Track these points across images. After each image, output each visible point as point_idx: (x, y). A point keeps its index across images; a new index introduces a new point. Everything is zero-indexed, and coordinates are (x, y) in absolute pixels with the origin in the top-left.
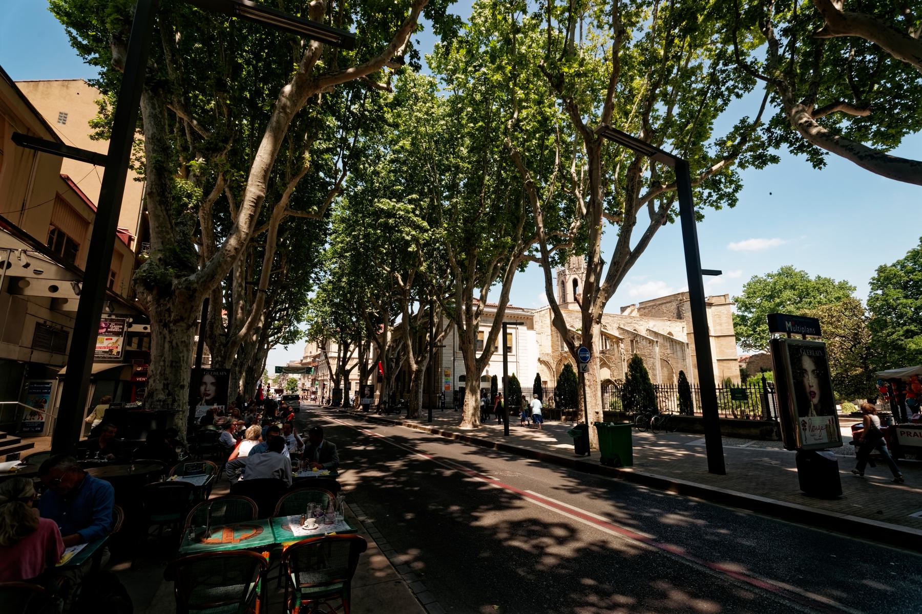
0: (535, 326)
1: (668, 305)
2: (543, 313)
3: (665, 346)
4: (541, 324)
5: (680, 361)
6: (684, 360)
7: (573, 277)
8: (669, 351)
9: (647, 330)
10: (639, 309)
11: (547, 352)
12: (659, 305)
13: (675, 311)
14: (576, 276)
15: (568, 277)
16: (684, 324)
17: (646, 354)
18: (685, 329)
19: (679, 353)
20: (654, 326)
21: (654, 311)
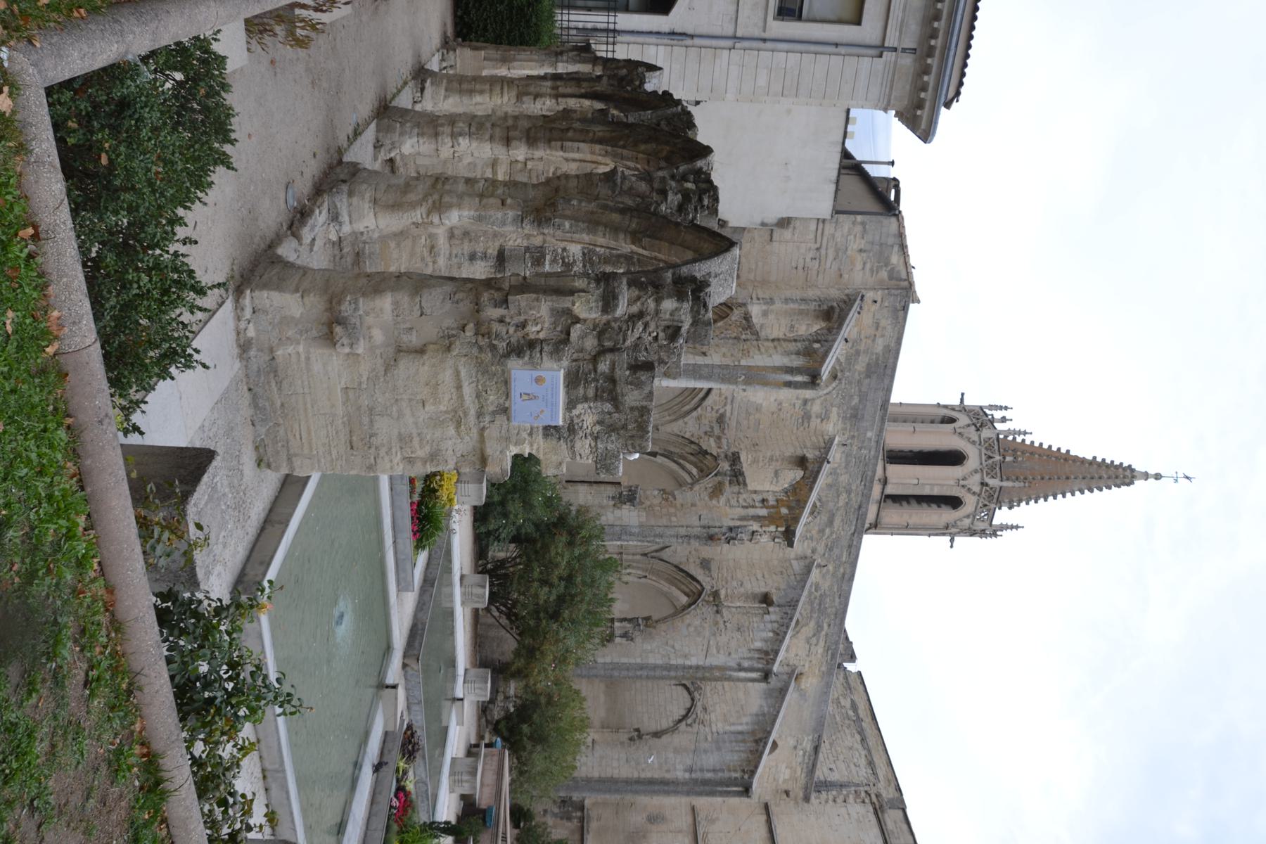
12: (861, 732)
14: (972, 462)
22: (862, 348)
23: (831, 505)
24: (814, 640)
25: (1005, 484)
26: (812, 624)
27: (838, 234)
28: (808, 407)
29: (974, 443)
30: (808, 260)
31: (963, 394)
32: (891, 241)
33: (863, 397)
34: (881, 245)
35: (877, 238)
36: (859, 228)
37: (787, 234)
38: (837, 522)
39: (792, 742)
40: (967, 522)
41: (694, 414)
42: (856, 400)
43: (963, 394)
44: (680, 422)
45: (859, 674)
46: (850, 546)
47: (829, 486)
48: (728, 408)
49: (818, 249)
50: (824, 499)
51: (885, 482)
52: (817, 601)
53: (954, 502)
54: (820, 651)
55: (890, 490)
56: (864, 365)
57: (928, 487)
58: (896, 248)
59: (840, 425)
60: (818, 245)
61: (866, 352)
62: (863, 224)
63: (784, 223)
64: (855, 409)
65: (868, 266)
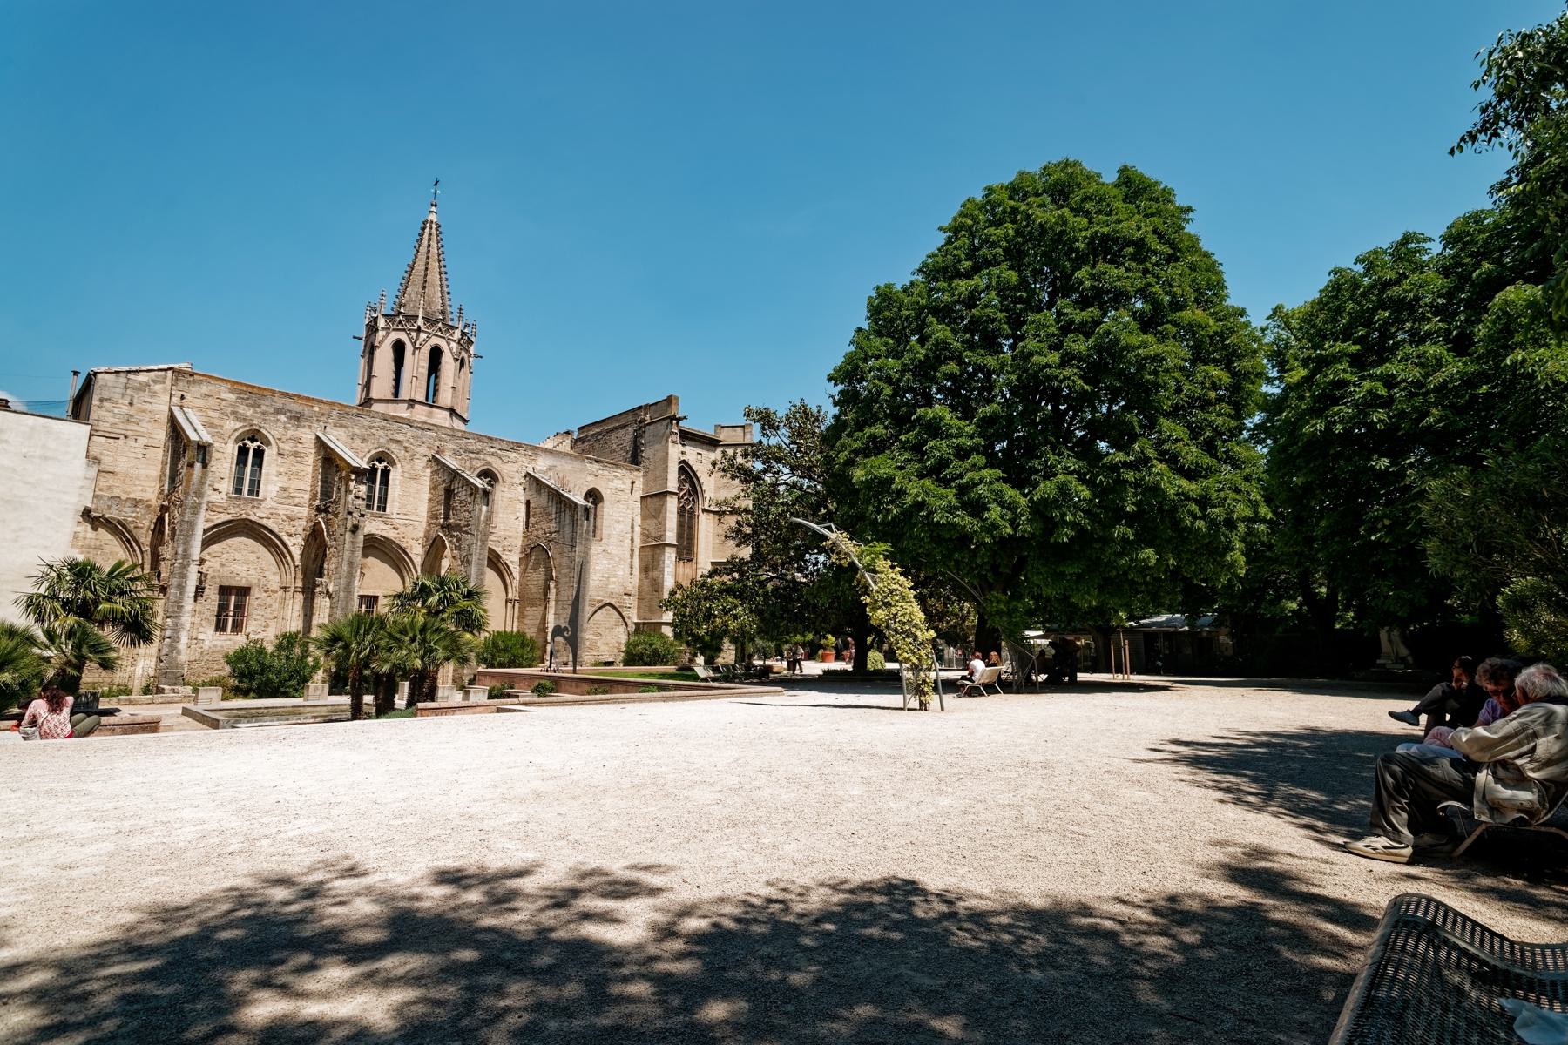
0: (95, 413)
1: (621, 432)
2: (142, 378)
3: (549, 514)
4: (126, 409)
5: (567, 549)
6: (573, 546)
7: (394, 336)
8: (553, 527)
9: (528, 475)
10: (574, 443)
11: (137, 495)
12: (609, 431)
13: (630, 448)
14: (403, 336)
15: (381, 334)
16: (638, 477)
17: (463, 523)
18: (639, 485)
19: (568, 530)
20: (551, 468)
21: (597, 446)
22: (230, 409)
23: (381, 440)
24: (505, 459)
25: (421, 315)
26: (489, 459)
27: (112, 420)
28: (285, 453)
29: (388, 334)
30: (136, 445)
31: (354, 337)
32: (122, 379)
33: (278, 411)
34: (126, 388)
35: (118, 390)
36: (107, 404)
37: (105, 460)
38: (400, 437)
39: (590, 478)
40: (454, 345)
41: (286, 538)
42: (283, 418)
43: (354, 337)
44: (292, 549)
45: (579, 429)
46: (423, 429)
47: (364, 440)
48: (281, 512)
49: (126, 437)
50: (376, 446)
51: (412, 403)
52: (470, 455)
53: (436, 354)
54: (515, 455)
55: (421, 397)
56: (247, 408)
57: (420, 370)
58: (131, 376)
59: (306, 430)
60: (122, 437)
61: (235, 407)
62: (101, 400)
63: (93, 459)
64: (290, 418)
65: (147, 400)
